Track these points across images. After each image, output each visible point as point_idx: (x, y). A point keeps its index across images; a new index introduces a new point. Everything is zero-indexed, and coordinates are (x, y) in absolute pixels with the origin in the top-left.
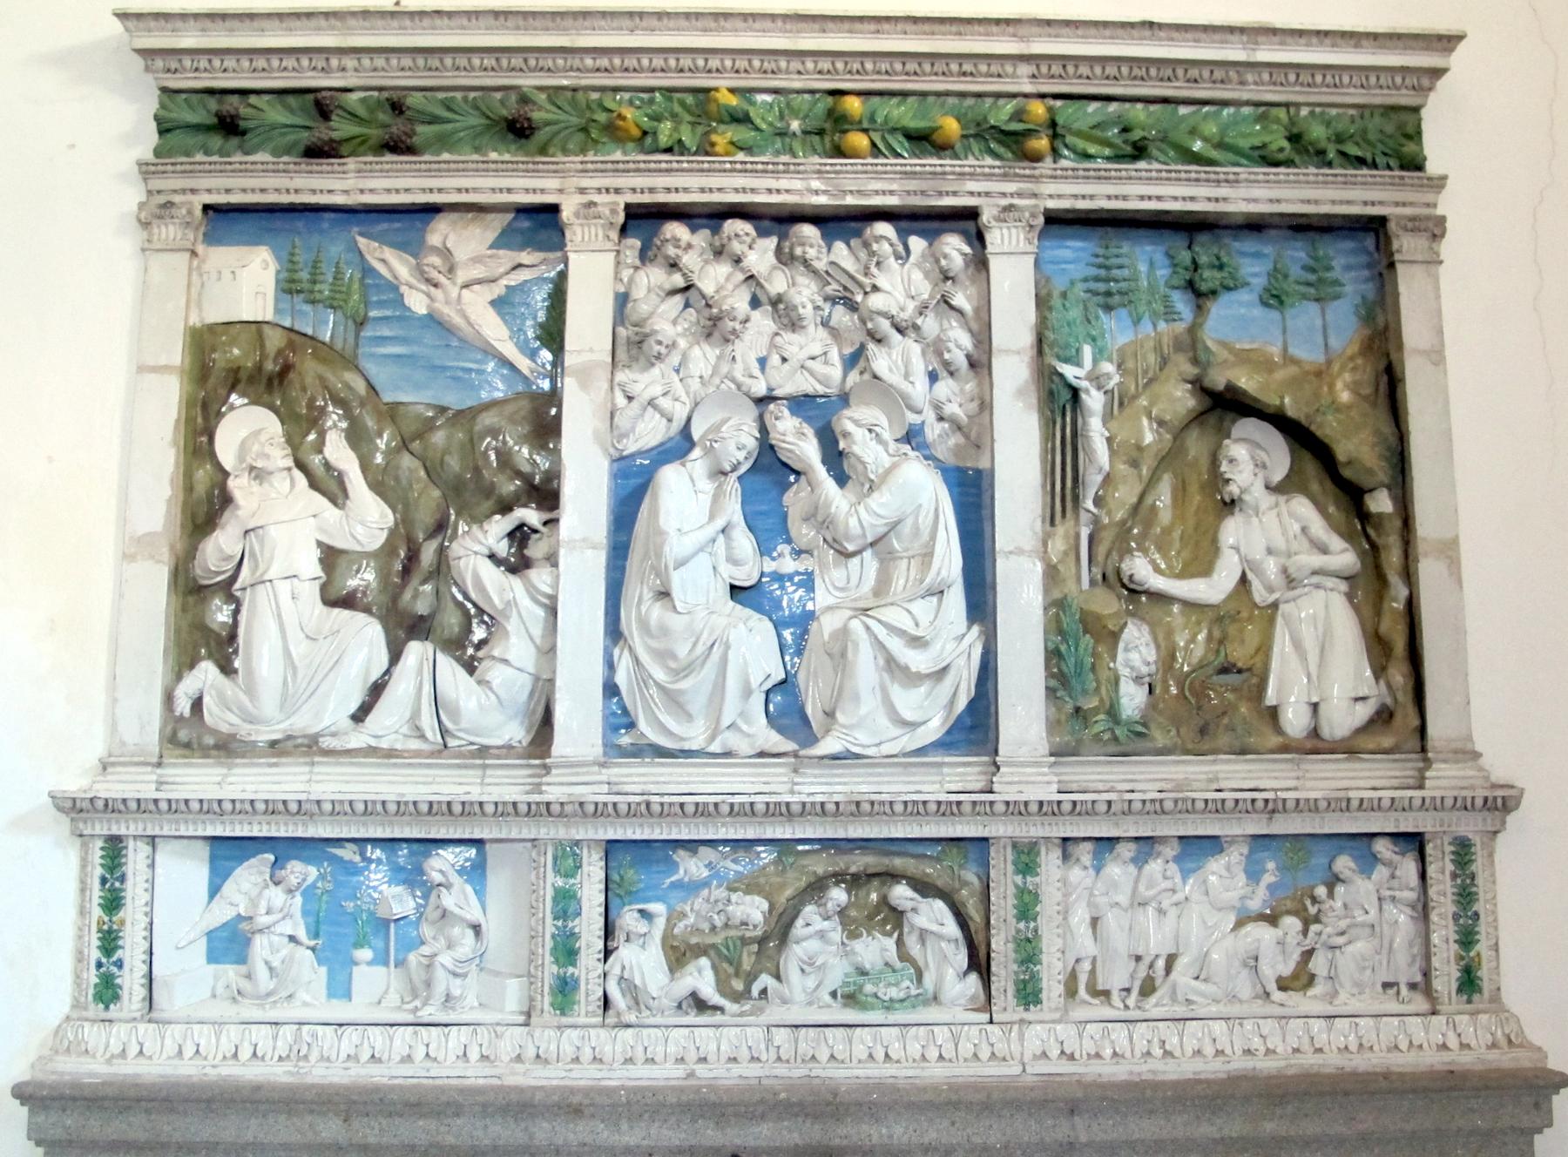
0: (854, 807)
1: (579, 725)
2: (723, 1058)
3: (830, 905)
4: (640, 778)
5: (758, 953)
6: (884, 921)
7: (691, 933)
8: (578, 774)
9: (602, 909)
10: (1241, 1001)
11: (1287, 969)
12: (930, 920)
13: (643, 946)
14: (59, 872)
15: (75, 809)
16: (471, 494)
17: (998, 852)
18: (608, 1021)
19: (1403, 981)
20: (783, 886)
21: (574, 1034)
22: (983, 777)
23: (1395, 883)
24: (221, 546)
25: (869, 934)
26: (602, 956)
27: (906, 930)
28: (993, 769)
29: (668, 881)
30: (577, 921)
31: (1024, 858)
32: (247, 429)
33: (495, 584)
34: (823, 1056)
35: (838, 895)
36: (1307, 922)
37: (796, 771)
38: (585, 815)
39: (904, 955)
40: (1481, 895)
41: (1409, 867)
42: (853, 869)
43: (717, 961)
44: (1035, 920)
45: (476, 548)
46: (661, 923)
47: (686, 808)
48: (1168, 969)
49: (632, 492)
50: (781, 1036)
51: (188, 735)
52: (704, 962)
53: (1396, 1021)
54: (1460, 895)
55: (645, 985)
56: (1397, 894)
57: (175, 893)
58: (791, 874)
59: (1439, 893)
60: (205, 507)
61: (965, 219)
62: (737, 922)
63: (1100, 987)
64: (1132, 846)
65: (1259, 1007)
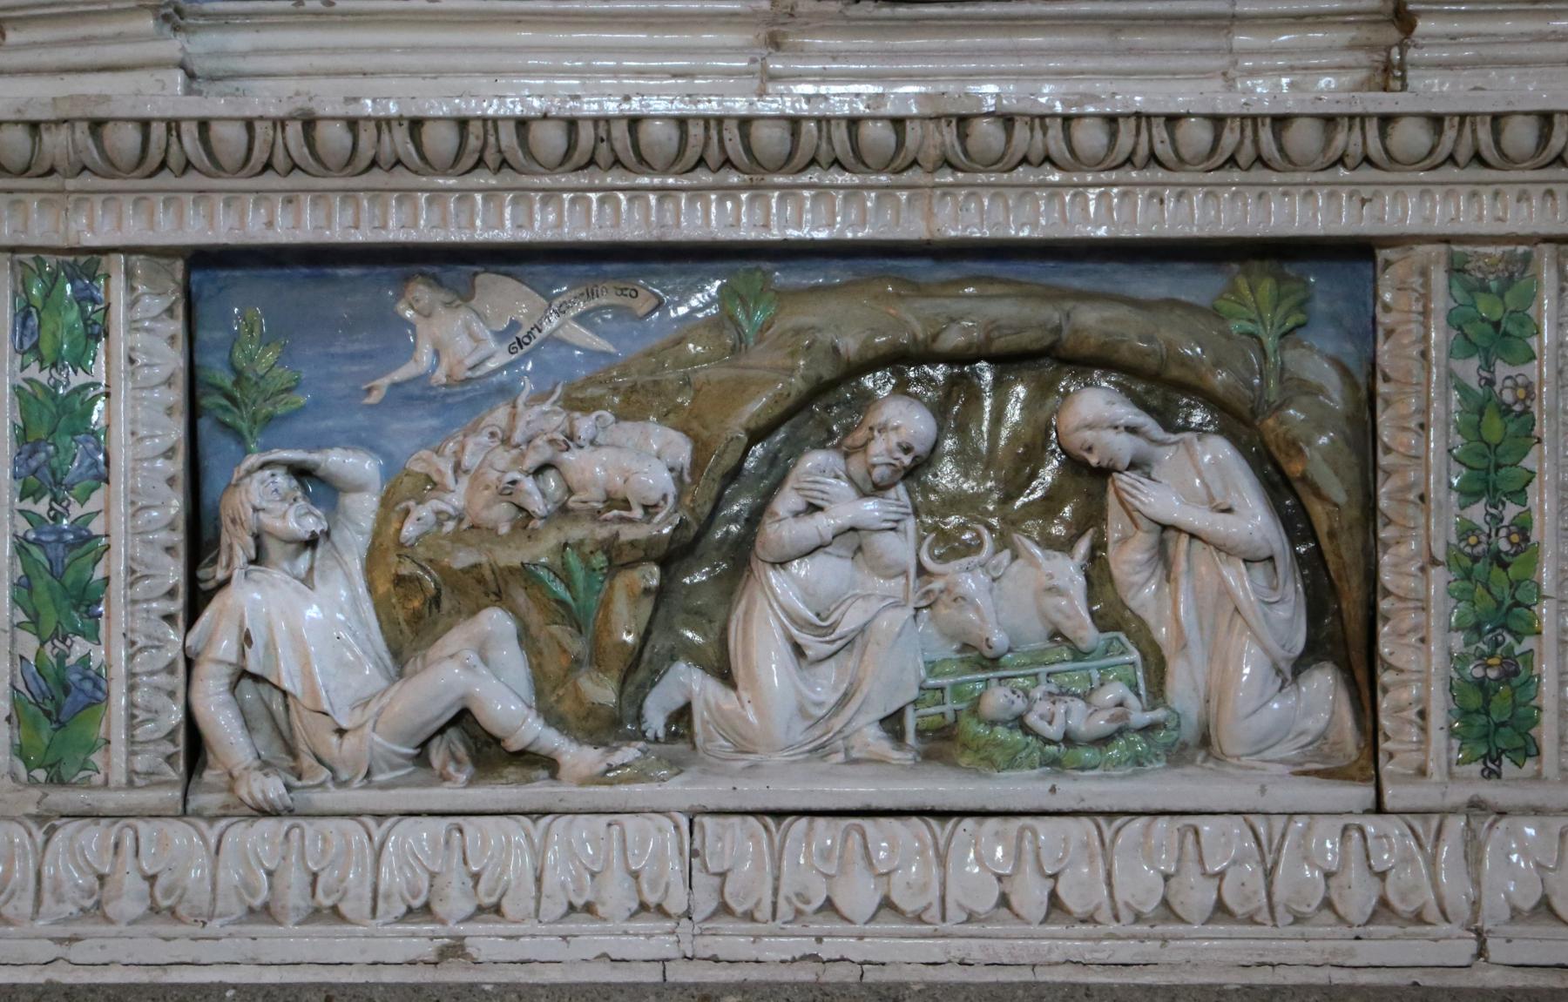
0: (950, 135)
2: (554, 907)
3: (880, 449)
5: (660, 595)
6: (1050, 505)
7: (456, 537)
8: (86, 41)
9: (178, 466)
12: (1189, 497)
13: (307, 580)
17: (1401, 289)
18: (199, 800)
20: (739, 390)
21: (93, 837)
22: (1362, 57)
25: (1003, 542)
26: (177, 606)
27: (1116, 526)
28: (1393, 34)
29: (384, 382)
30: (96, 501)
31: (1486, 307)
34: (859, 896)
35: (903, 420)
37: (775, 43)
38: (112, 168)
39: (1111, 613)
42: (953, 339)
43: (535, 618)
44: (1519, 495)
46: (363, 508)
47: (429, 134)
50: (738, 848)
52: (496, 621)
55: (314, 694)
58: (761, 358)
62: (595, 496)
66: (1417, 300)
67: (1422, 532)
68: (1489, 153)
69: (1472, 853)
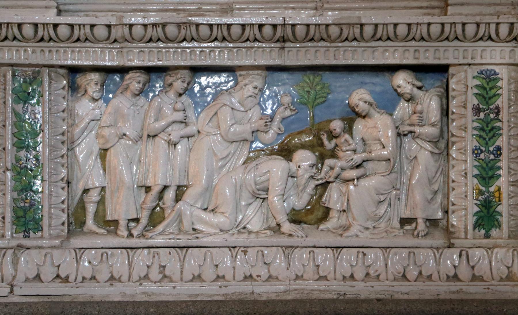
10: (250, 232)
11: (299, 202)
19: (420, 215)
23: (415, 118)
36: (322, 158)
40: (504, 132)
41: (431, 104)
48: (178, 198)
53: (405, 253)
54: (482, 129)
56: (418, 130)
59: (460, 128)
63: (109, 218)
64: (141, 77)
65: (268, 238)
66: (2, 85)
67: (3, 160)
68: (19, 36)
69: (15, 262)
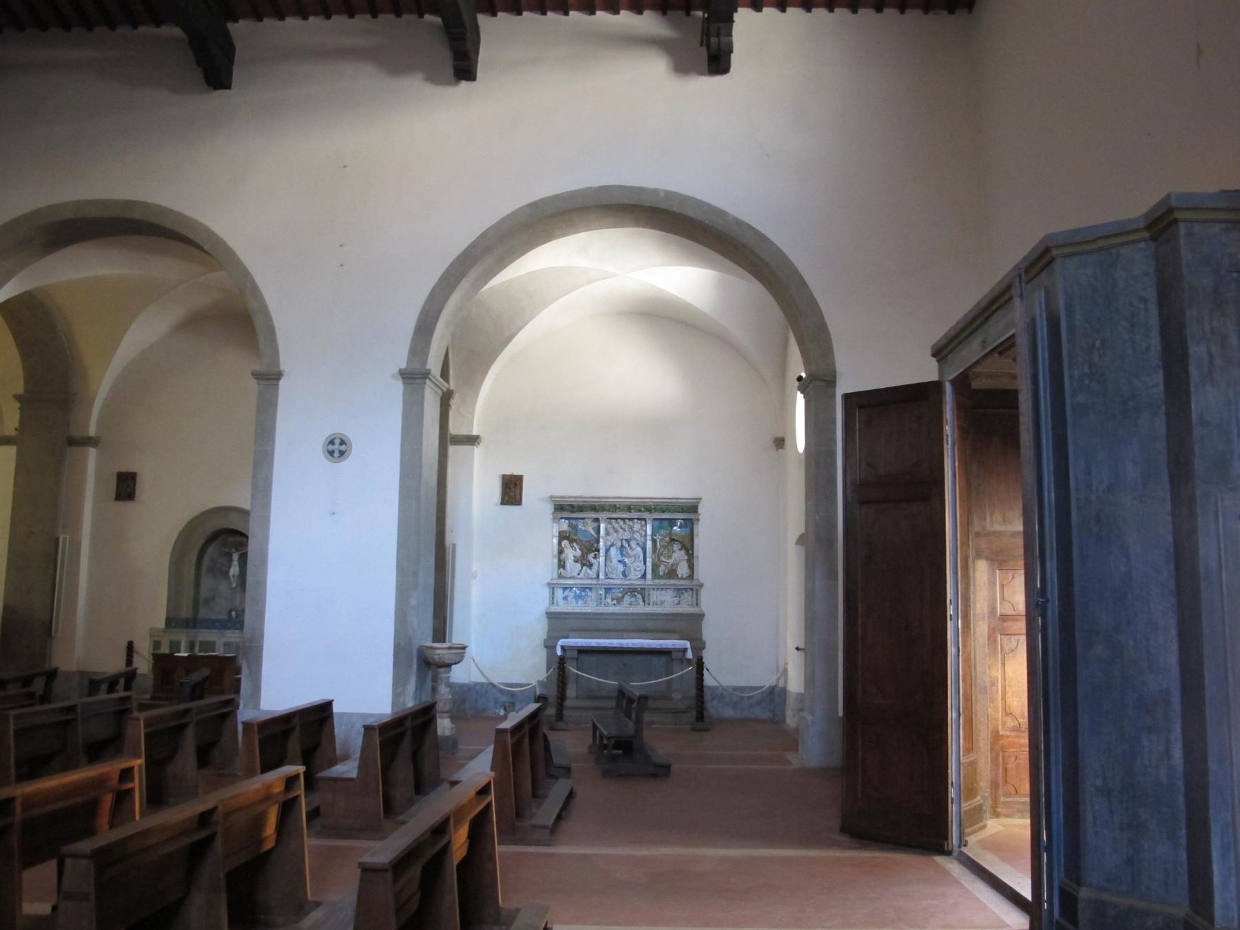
1: (602, 576)
4: (608, 581)
14: (547, 591)
15: (549, 584)
16: (590, 551)
24: (563, 556)
32: (565, 543)
33: (593, 560)
45: (591, 556)
49: (607, 551)
51: (560, 576)
57: (559, 593)
60: (561, 552)
61: (645, 520)
